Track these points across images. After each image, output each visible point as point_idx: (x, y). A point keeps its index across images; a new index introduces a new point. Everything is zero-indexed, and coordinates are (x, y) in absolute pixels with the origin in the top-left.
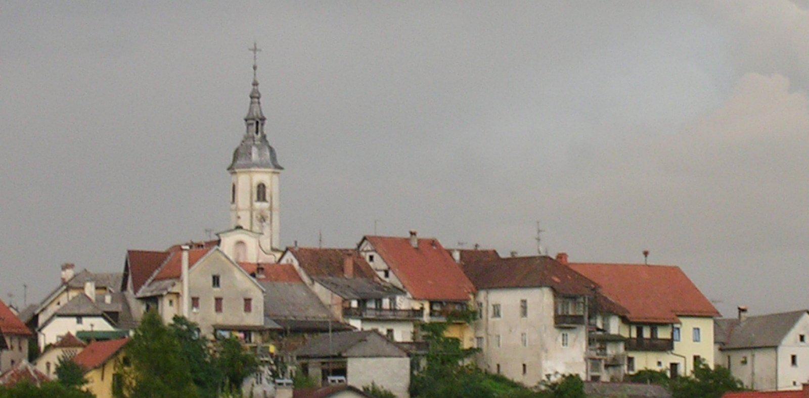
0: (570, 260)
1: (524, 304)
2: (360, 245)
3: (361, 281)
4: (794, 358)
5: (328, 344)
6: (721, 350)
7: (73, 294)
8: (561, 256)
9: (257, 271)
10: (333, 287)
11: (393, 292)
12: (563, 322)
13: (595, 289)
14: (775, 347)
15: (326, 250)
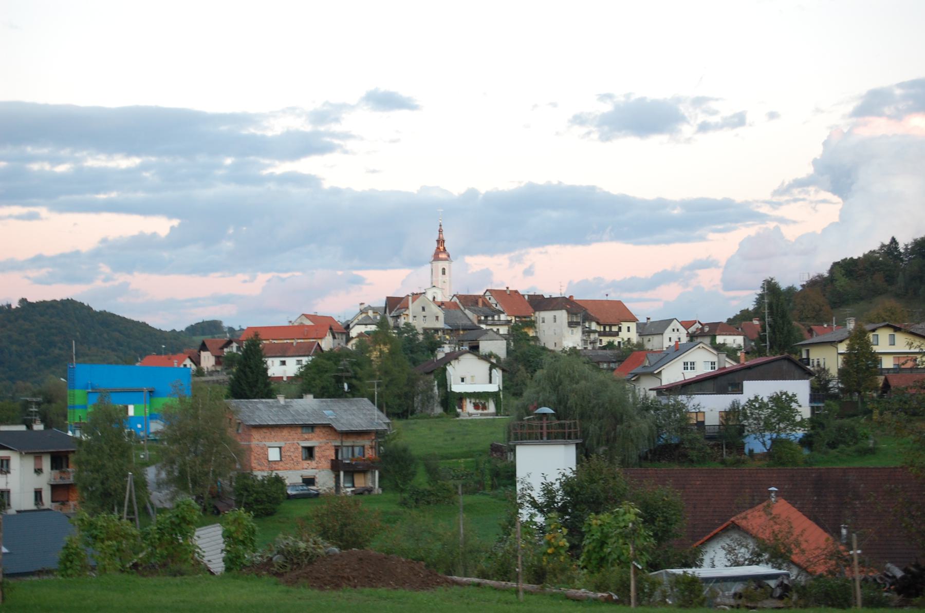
0: (574, 298)
1: (555, 318)
2: (485, 293)
3: (485, 308)
4: (670, 338)
5: (472, 335)
6: (639, 335)
7: (364, 315)
8: (571, 297)
9: (440, 305)
10: (474, 311)
11: (499, 312)
12: (571, 324)
13: (585, 310)
14: (662, 334)
15: (471, 296)
